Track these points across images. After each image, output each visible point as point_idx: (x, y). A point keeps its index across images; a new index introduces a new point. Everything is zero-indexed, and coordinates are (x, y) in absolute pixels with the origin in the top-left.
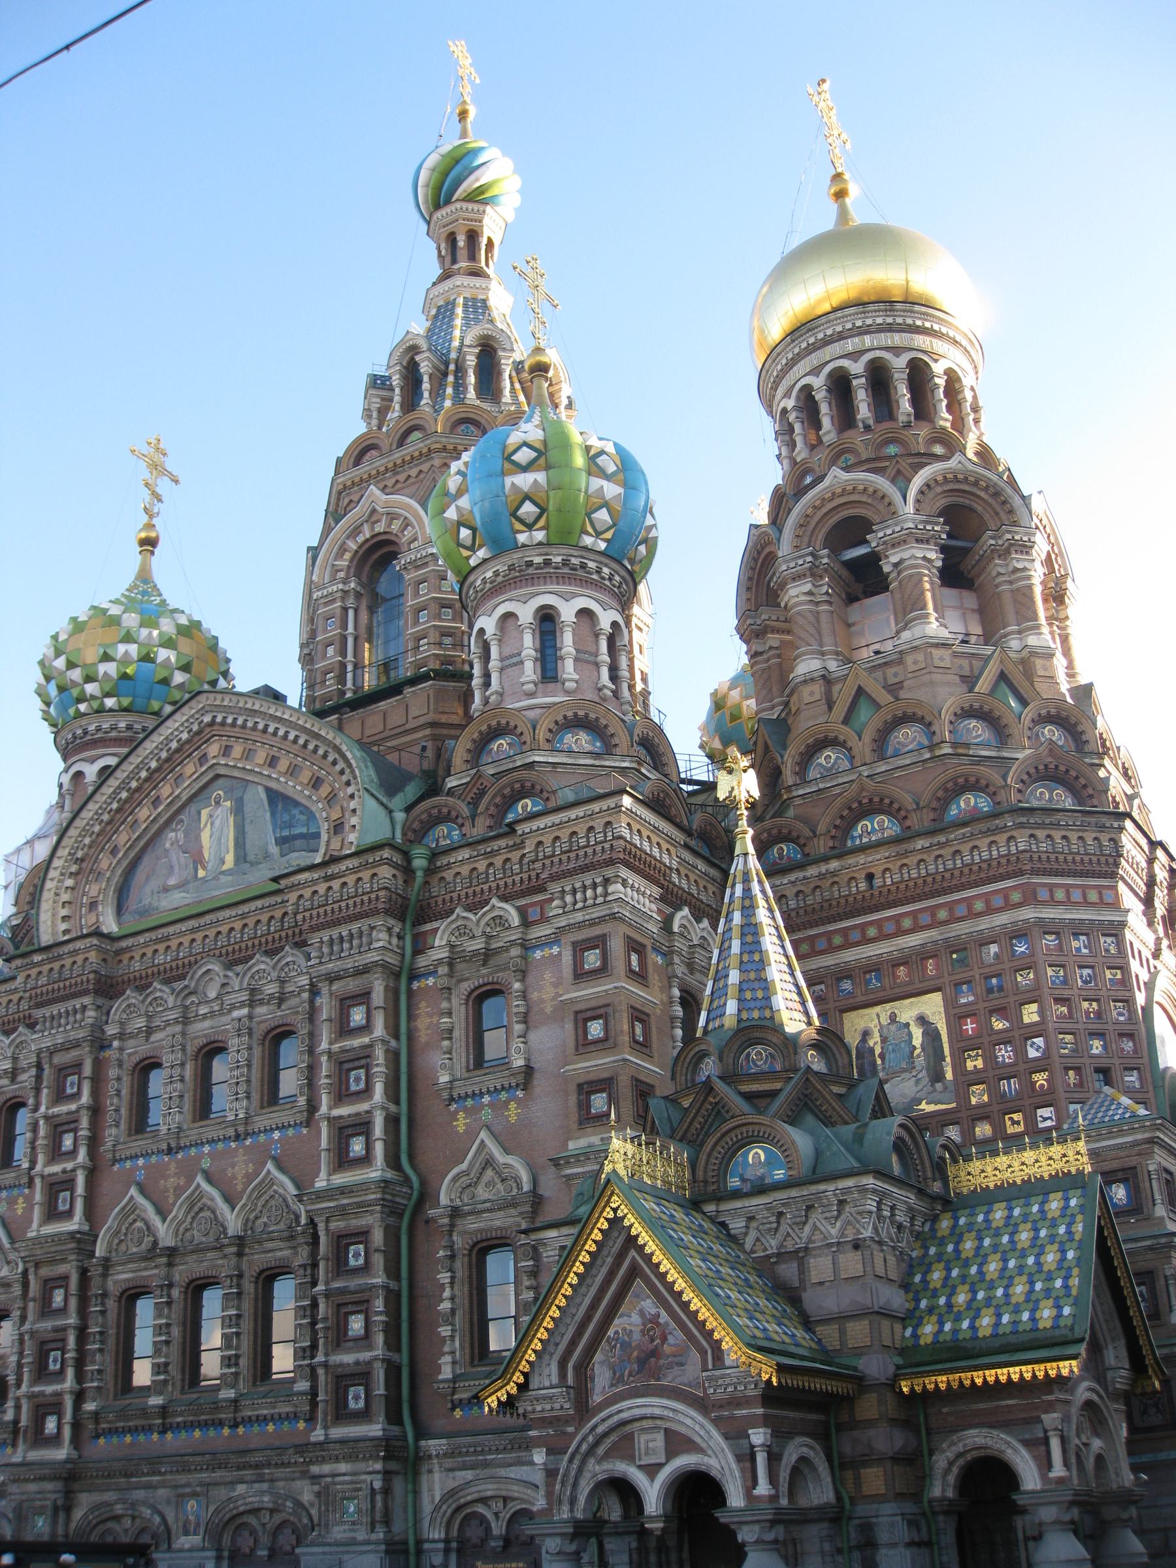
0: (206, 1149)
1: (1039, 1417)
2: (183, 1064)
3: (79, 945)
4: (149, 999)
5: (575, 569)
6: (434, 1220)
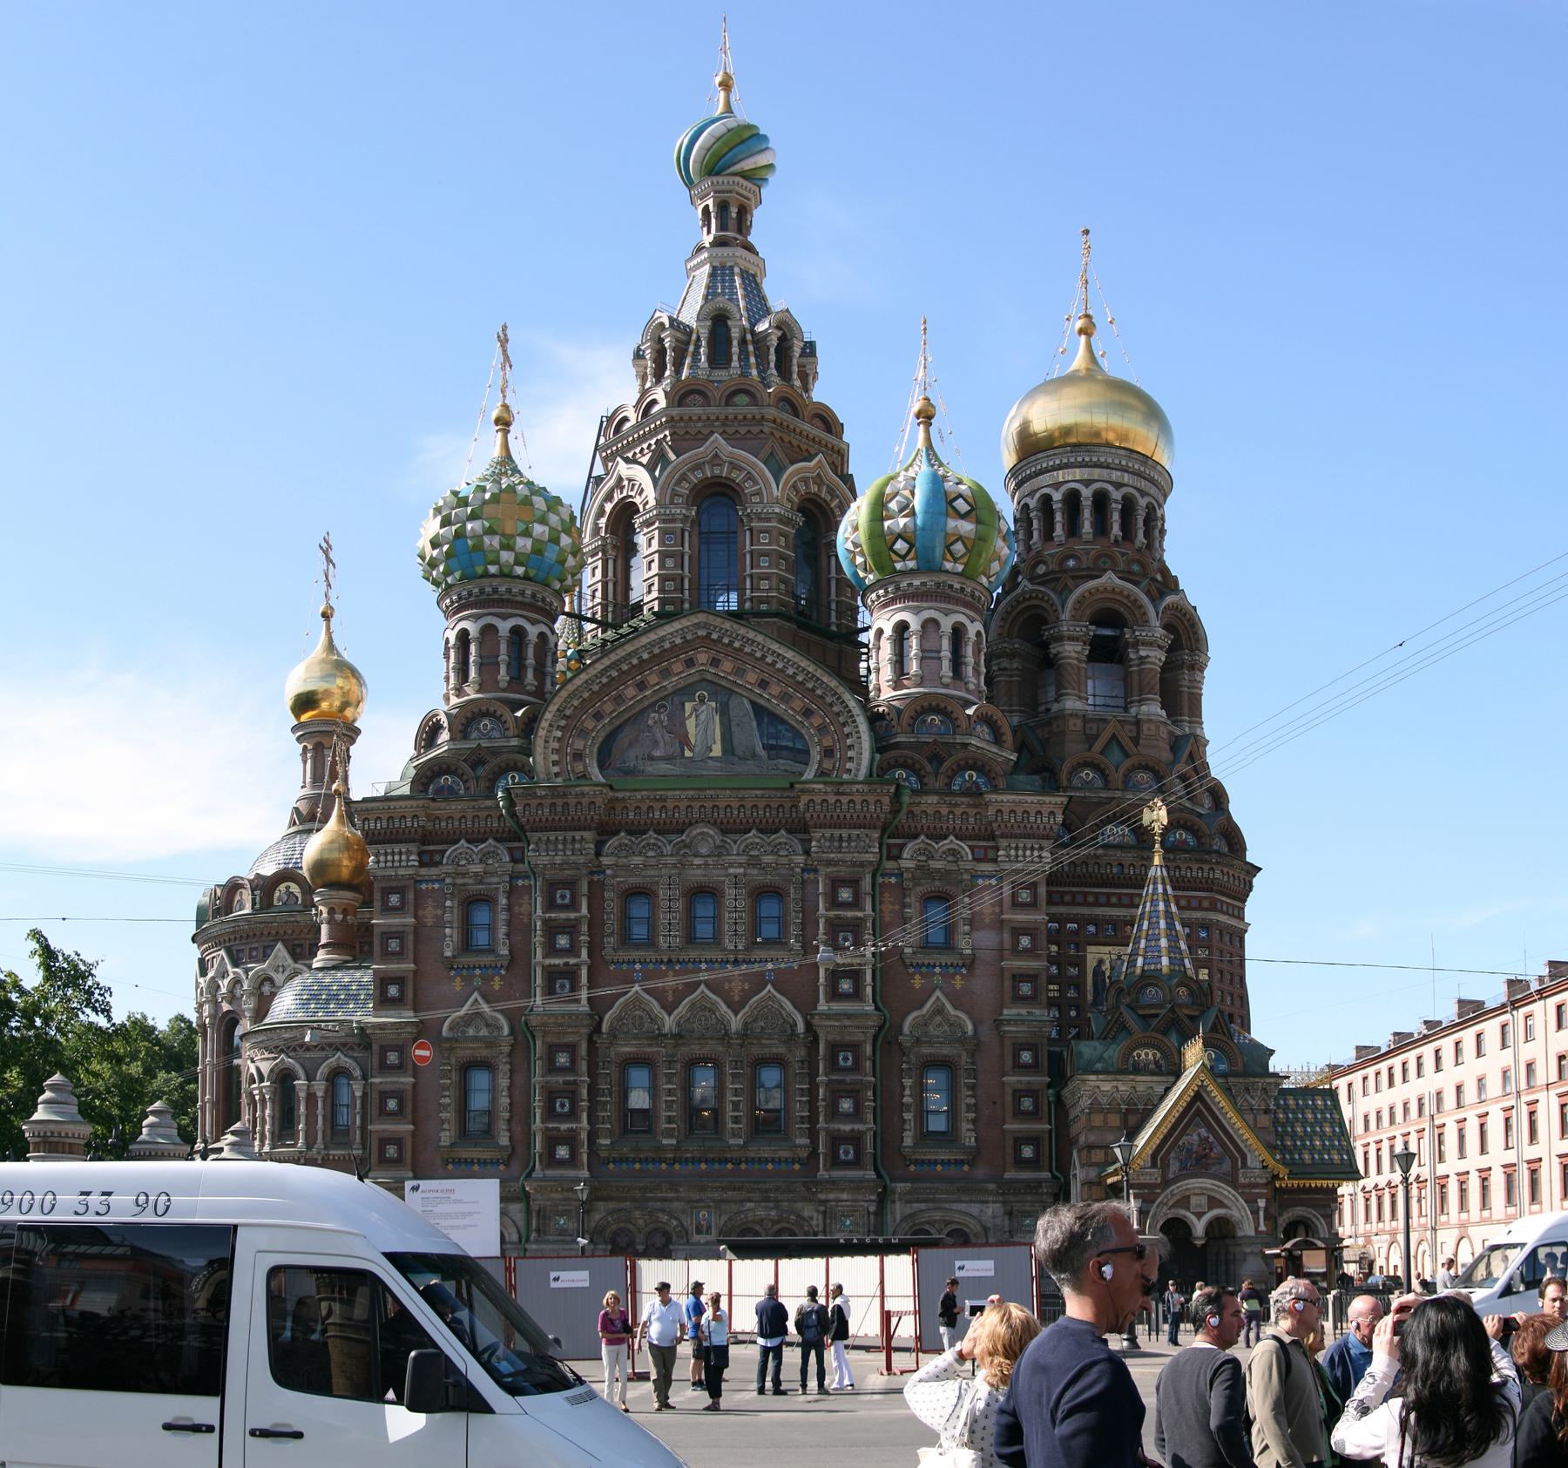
6: (900, 1044)
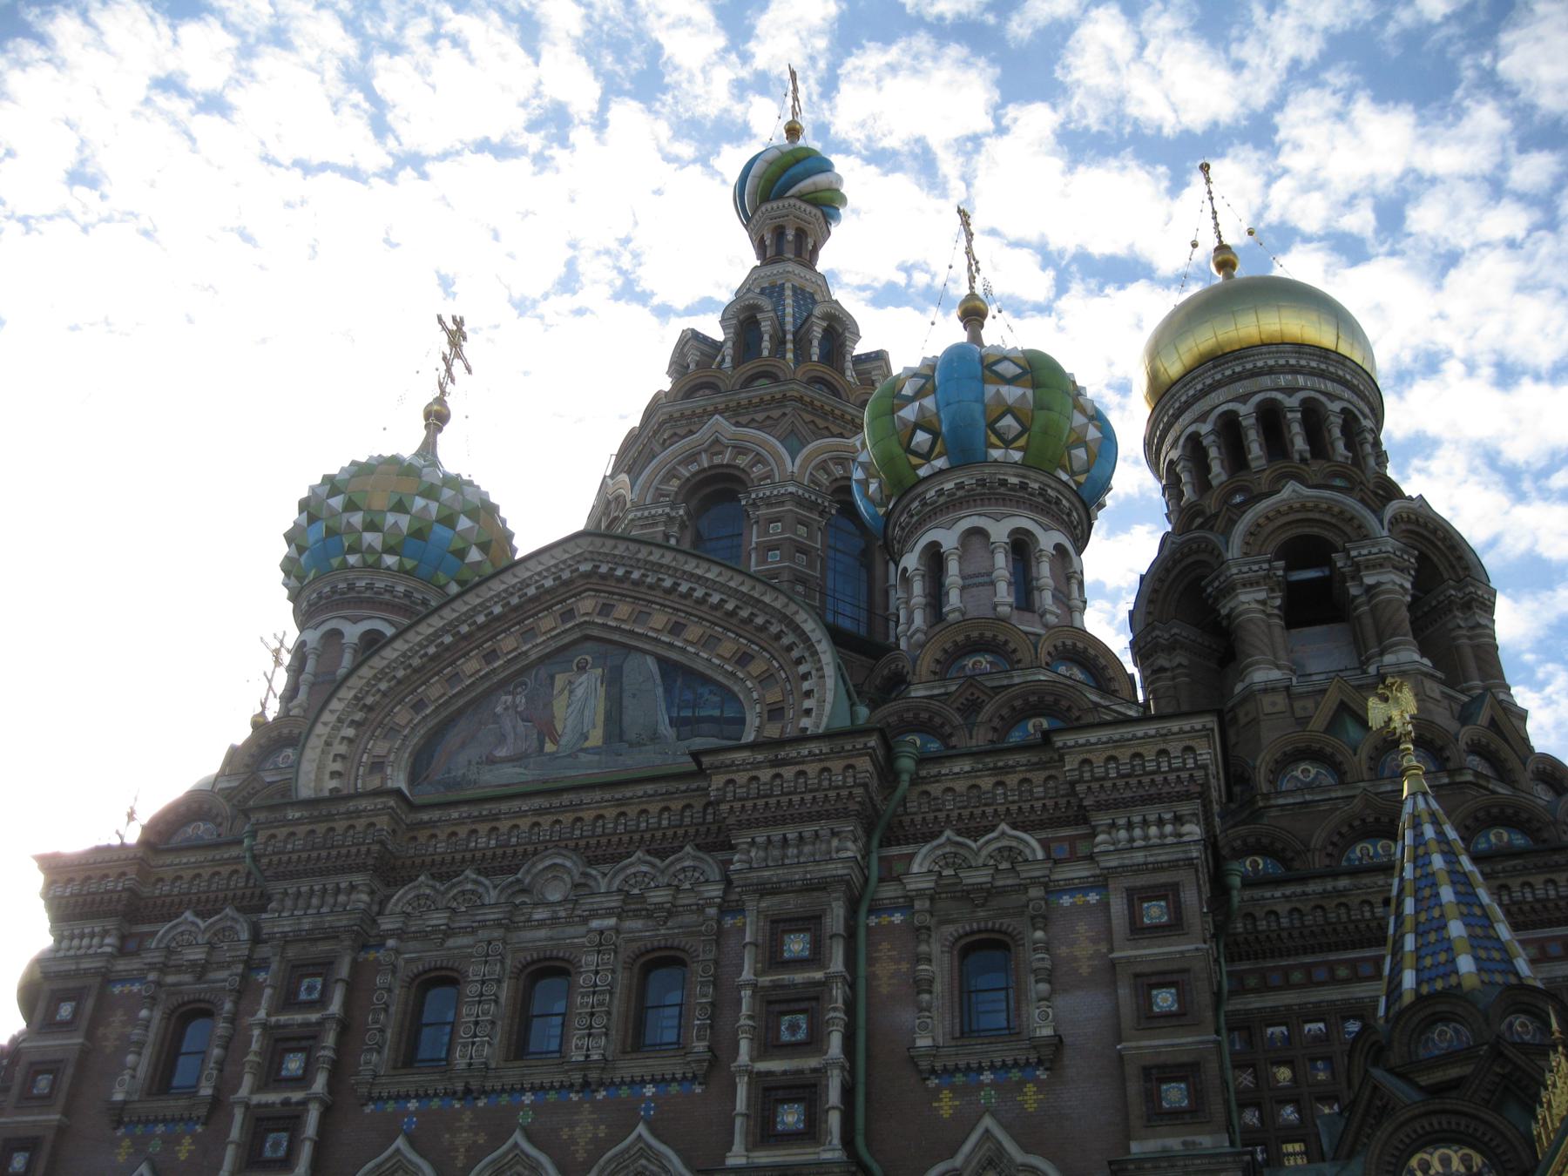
0: (528, 1098)
2: (499, 981)
3: (364, 804)
4: (455, 891)
5: (1050, 502)
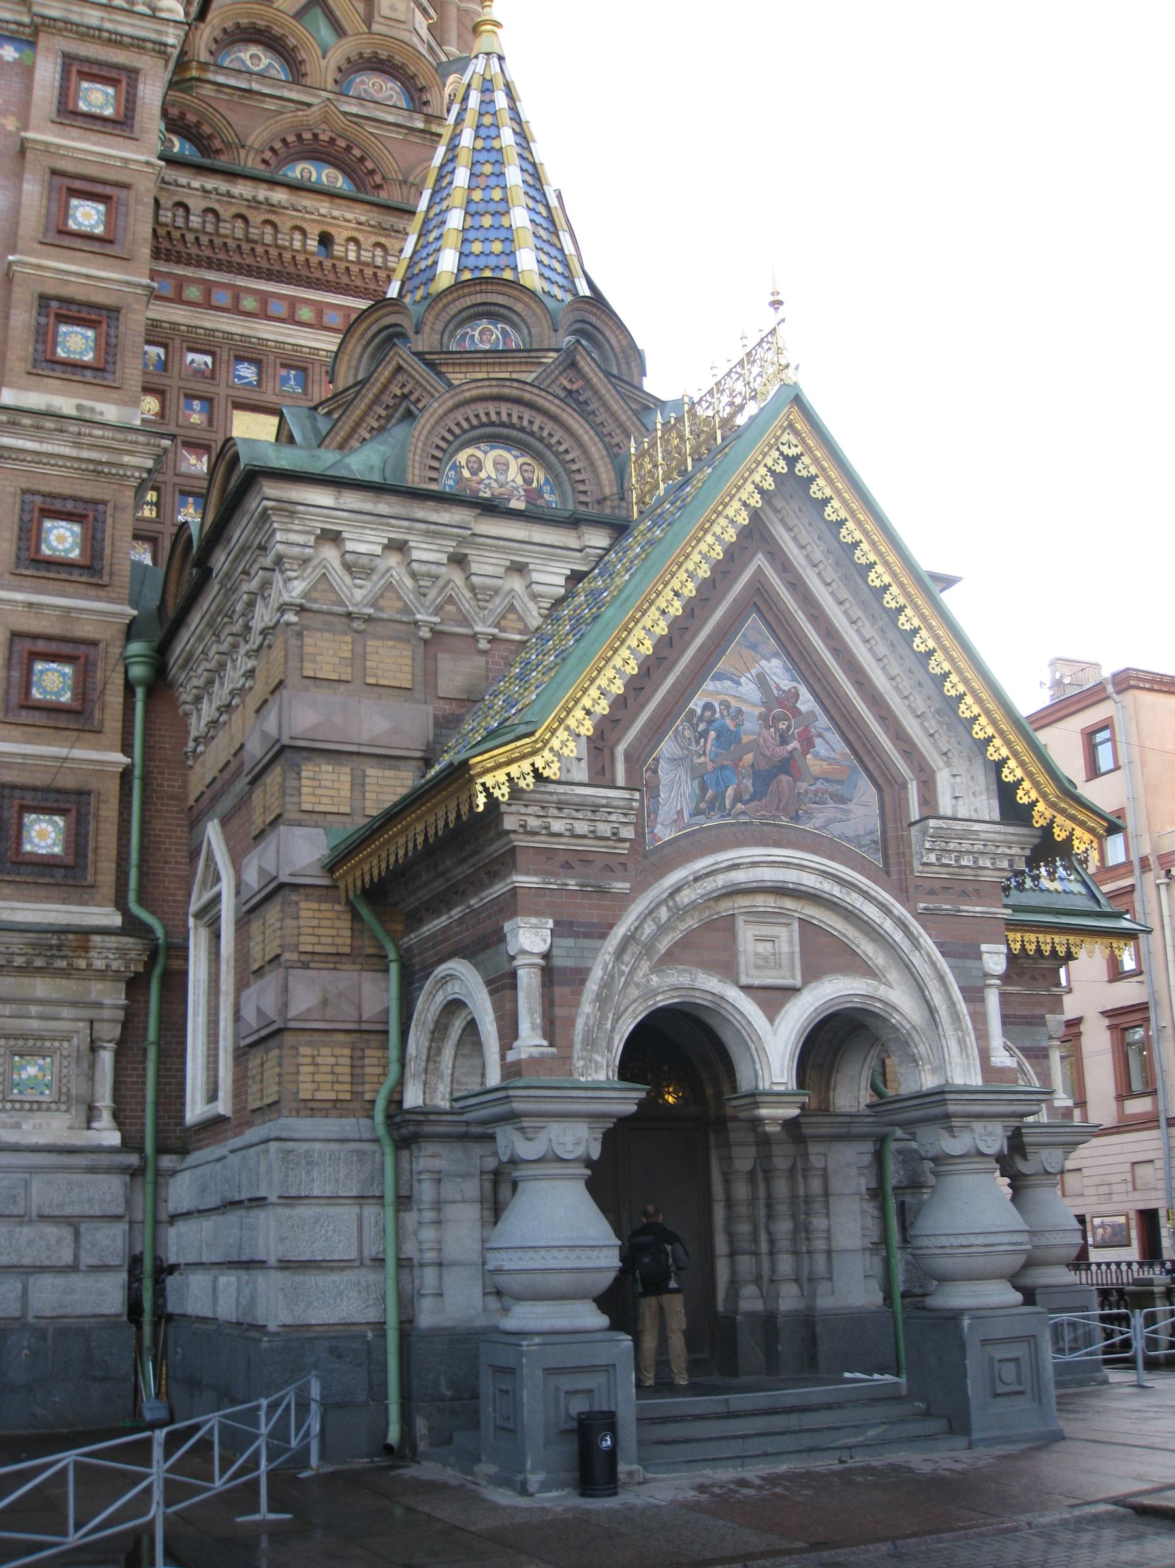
1: (1043, 1017)
